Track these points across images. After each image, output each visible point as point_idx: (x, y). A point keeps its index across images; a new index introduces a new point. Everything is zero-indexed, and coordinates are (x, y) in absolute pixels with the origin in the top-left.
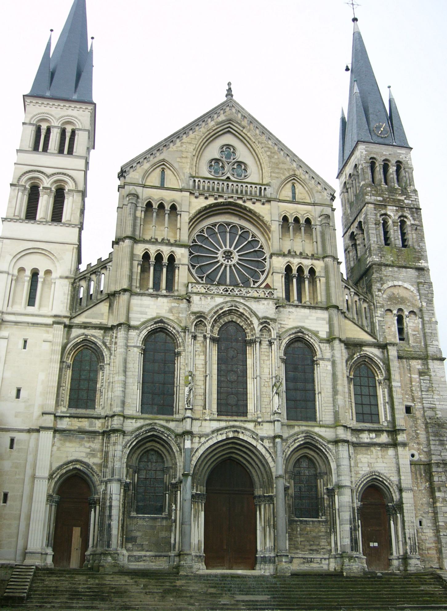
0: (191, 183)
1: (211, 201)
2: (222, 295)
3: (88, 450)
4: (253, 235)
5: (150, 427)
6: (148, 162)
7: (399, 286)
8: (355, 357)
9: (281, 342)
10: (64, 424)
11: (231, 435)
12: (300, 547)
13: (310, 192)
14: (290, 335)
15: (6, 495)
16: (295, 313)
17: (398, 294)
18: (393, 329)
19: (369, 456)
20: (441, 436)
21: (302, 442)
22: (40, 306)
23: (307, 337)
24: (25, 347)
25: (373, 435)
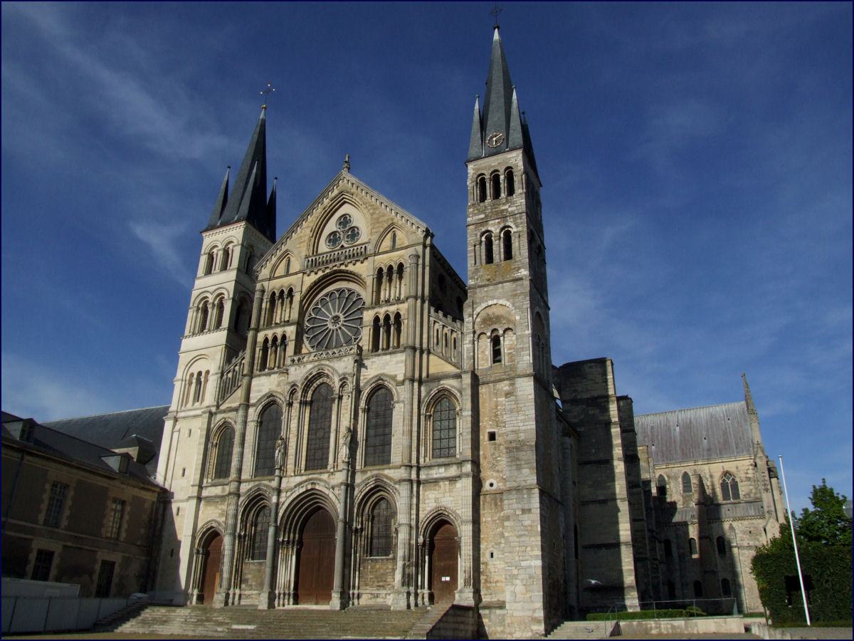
1: (320, 274)
3: (220, 511)
7: (495, 304)
8: (433, 393)
11: (309, 487)
16: (378, 362)
17: (493, 313)
19: (436, 492)
20: (518, 459)
21: (372, 486)
22: (203, 400)
25: (442, 470)
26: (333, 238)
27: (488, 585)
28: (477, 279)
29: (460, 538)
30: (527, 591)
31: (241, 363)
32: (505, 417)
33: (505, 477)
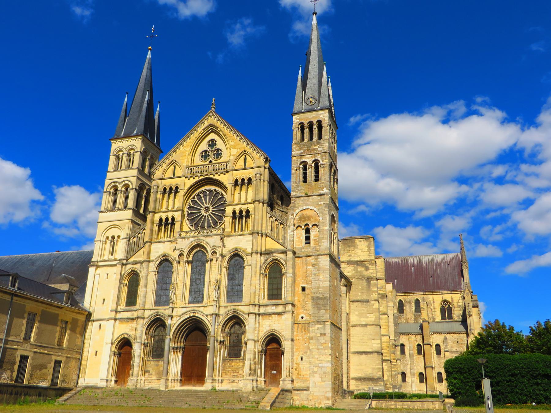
0: (187, 170)
1: (197, 179)
2: (192, 237)
4: (221, 194)
5: (156, 314)
6: (165, 163)
7: (308, 209)
9: (225, 258)
10: (119, 316)
11: (192, 315)
12: (229, 374)
13: (253, 159)
14: (231, 253)
15: (97, 352)
17: (306, 214)
18: (301, 238)
20: (319, 304)
21: (231, 315)
23: (240, 253)
24: (107, 278)
25: (274, 307)
26: (205, 155)
27: (299, 376)
28: (297, 192)
29: (284, 349)
30: (322, 381)
31: (142, 232)
32: (311, 278)
33: (310, 313)
